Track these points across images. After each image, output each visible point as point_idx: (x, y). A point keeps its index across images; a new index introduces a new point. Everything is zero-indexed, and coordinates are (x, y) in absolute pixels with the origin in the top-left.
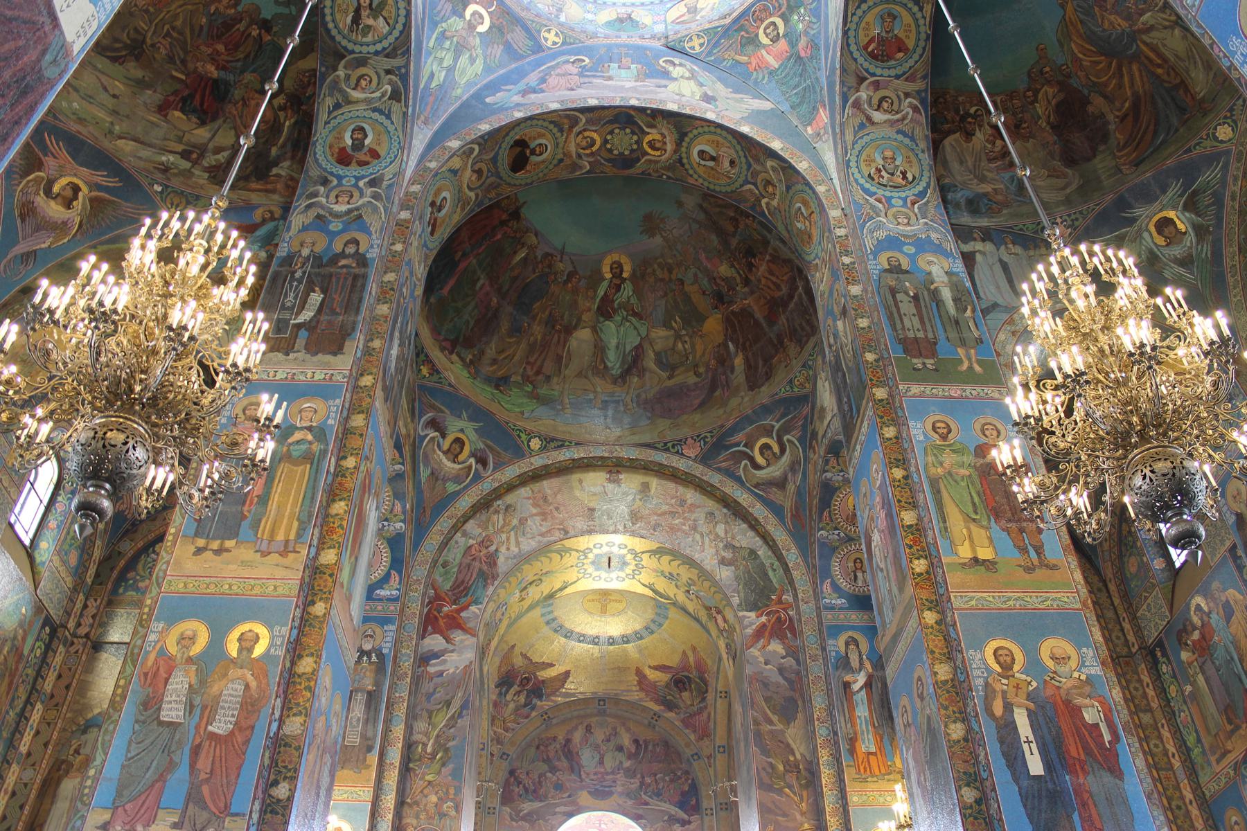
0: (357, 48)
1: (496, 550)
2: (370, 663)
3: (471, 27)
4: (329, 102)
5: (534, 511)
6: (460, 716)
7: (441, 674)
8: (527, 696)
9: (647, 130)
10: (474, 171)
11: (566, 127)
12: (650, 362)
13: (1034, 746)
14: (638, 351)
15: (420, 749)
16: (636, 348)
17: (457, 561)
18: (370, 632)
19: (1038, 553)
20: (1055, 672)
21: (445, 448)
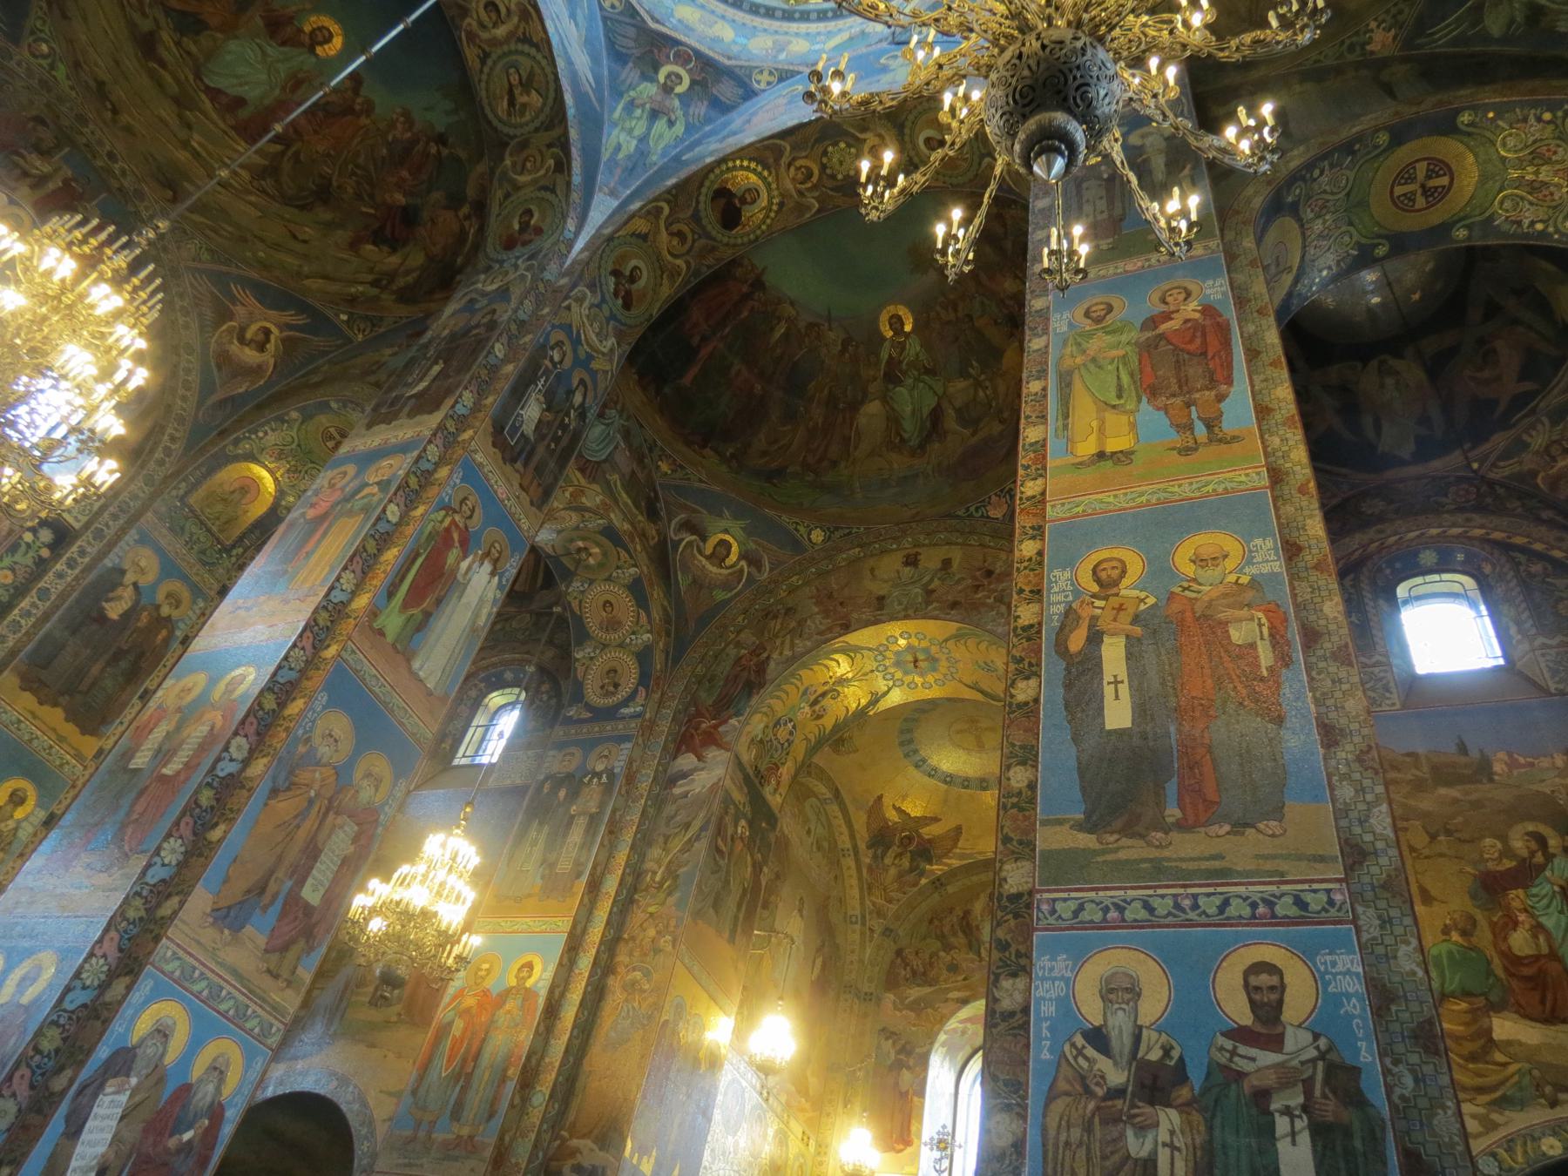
0: (518, 132)
1: (768, 658)
2: (600, 784)
3: (667, 89)
4: (499, 194)
5: (816, 610)
6: (698, 838)
7: (685, 795)
8: (912, 860)
9: (862, 136)
10: (671, 234)
11: (771, 161)
12: (950, 422)
13: (1124, 689)
14: (936, 415)
15: (648, 879)
16: (934, 410)
17: (725, 673)
18: (606, 753)
19: (1209, 426)
20: (1194, 580)
21: (709, 550)
